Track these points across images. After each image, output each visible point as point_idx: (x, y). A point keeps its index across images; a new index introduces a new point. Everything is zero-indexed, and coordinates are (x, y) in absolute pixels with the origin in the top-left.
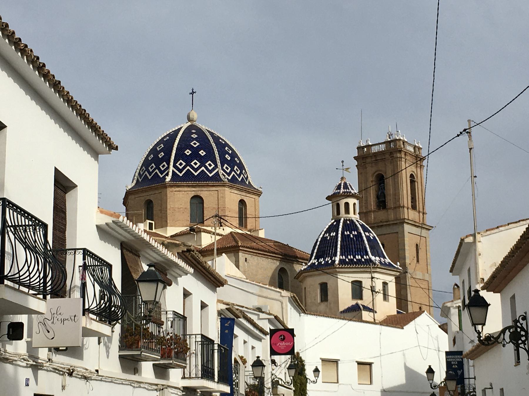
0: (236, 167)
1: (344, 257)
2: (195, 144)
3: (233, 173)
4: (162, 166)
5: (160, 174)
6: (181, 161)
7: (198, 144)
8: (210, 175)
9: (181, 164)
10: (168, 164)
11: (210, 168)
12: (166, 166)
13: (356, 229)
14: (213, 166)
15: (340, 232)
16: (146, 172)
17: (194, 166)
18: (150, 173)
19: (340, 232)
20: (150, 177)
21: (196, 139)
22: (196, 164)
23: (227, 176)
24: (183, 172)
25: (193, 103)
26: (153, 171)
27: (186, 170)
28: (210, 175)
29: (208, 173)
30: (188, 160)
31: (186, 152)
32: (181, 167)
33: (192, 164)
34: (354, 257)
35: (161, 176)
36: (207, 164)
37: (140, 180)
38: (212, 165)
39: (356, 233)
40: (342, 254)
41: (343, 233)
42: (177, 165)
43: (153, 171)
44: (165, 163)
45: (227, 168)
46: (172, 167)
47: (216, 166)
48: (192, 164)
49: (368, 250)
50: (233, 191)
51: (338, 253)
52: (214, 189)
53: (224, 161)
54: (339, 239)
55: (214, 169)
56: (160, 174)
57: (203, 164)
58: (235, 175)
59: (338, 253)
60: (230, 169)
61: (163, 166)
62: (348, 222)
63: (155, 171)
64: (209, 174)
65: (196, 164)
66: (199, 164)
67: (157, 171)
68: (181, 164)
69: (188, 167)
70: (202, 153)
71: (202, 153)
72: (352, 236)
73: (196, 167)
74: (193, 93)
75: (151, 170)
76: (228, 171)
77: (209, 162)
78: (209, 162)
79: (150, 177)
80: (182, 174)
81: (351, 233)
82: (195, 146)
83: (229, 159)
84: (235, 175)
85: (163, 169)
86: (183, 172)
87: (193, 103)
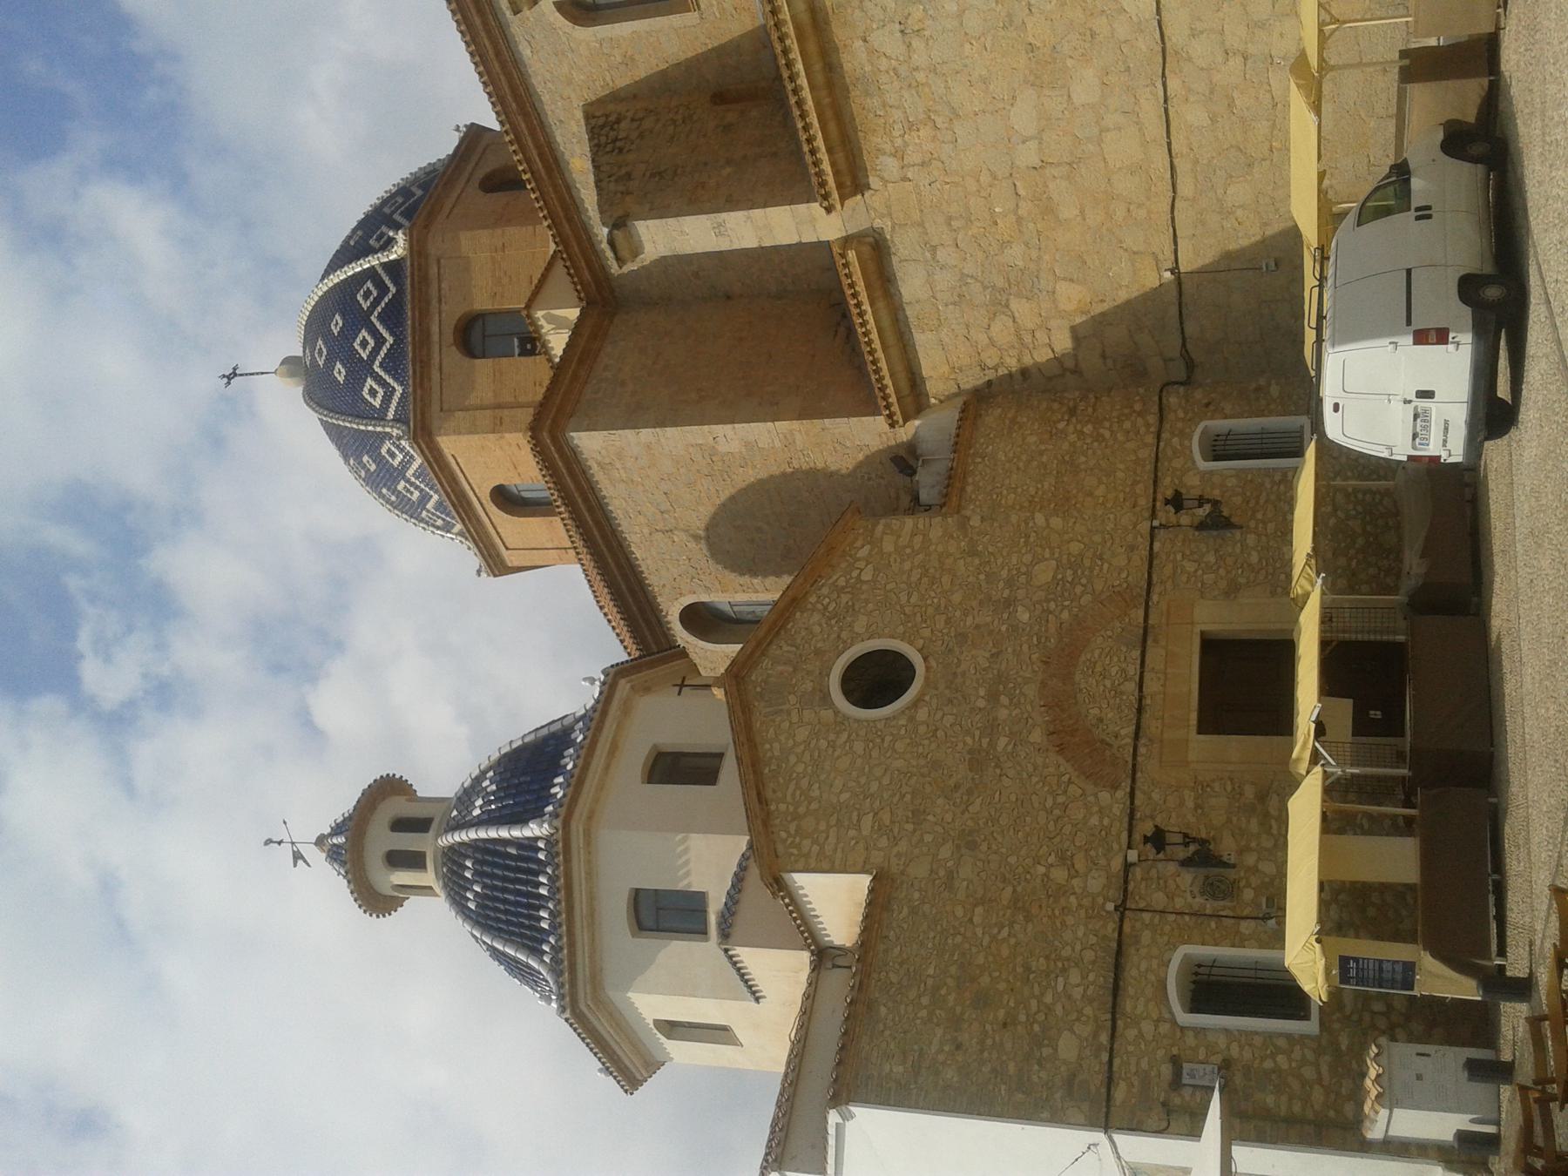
3: (397, 217)
5: (415, 466)
8: (393, 289)
14: (369, 284)
17: (369, 348)
18: (425, 498)
20: (436, 497)
26: (417, 487)
27: (382, 373)
28: (393, 289)
29: (386, 300)
31: (341, 379)
38: (368, 288)
42: (377, 403)
43: (417, 487)
47: (371, 273)
50: (446, 209)
52: (433, 270)
56: (415, 466)
58: (402, 208)
60: (384, 228)
63: (413, 479)
64: (390, 295)
66: (364, 333)
67: (409, 473)
68: (373, 393)
73: (372, 343)
75: (416, 494)
80: (396, 385)
84: (402, 208)
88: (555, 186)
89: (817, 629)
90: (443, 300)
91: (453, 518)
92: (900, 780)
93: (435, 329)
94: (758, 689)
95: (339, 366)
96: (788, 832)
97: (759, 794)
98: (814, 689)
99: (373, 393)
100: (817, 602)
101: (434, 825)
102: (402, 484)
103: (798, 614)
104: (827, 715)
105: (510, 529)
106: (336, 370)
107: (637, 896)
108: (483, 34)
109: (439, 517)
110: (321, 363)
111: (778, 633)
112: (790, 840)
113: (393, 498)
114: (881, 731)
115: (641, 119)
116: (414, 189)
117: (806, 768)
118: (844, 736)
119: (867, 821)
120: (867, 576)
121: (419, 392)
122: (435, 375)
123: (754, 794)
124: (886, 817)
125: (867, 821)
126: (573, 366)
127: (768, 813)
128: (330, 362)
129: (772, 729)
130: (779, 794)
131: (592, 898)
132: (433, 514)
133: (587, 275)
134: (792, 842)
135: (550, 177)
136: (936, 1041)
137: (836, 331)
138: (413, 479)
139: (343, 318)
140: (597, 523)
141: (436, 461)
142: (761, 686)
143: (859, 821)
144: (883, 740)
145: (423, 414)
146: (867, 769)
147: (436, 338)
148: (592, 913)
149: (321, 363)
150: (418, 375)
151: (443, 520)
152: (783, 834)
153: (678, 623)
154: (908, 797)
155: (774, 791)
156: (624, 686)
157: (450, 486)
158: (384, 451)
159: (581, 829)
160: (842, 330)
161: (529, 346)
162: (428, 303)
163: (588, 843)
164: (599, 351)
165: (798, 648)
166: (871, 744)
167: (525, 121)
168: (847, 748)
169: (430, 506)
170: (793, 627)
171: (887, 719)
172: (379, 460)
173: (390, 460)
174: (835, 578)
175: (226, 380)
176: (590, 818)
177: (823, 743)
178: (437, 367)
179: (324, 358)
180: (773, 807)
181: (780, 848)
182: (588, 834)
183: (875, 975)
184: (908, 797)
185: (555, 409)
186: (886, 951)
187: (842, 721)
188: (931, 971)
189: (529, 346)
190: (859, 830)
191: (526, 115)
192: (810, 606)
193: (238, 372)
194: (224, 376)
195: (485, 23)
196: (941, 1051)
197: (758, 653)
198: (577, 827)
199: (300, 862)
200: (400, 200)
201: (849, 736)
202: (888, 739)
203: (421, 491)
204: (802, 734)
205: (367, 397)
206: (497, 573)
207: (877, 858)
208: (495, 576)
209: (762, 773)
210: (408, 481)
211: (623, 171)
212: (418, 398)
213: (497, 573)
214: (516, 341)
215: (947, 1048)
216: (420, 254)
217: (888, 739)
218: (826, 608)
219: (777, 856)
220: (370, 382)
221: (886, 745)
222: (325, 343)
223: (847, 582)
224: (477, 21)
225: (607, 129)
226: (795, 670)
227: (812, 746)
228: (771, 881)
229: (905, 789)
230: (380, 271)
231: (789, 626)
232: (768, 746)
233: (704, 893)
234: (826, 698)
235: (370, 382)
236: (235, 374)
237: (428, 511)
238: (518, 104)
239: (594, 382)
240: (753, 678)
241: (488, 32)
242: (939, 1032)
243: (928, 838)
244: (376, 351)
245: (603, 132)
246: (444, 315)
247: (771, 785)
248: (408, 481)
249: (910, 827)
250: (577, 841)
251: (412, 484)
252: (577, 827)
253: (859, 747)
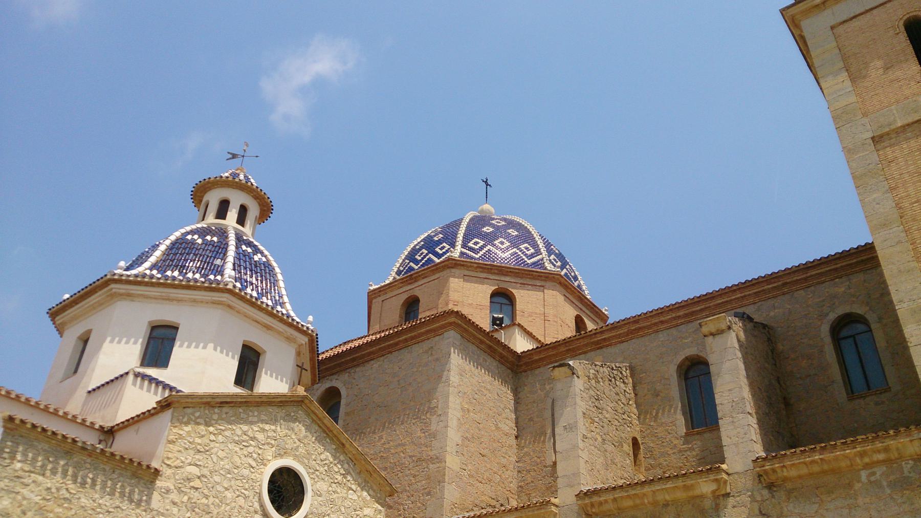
0: (568, 267)
2: (497, 222)
4: (439, 249)
7: (504, 223)
9: (476, 243)
14: (532, 251)
18: (416, 262)
20: (416, 267)
24: (481, 253)
25: (487, 195)
26: (423, 259)
30: (489, 239)
31: (484, 229)
42: (471, 244)
43: (423, 259)
46: (460, 246)
47: (538, 252)
48: (496, 242)
63: (428, 257)
64: (526, 259)
65: (502, 243)
67: (430, 255)
70: (514, 233)
75: (419, 258)
78: (526, 245)
80: (479, 255)
86: (481, 253)
87: (487, 195)
88: (586, 345)
89: (323, 457)
90: (522, 285)
91: (405, 273)
92: (218, 497)
93: (507, 279)
94: (292, 414)
95: (491, 230)
96: (198, 417)
97: (227, 403)
98: (287, 449)
99: (476, 243)
100: (340, 460)
101: (240, 227)
102: (427, 252)
103: (334, 447)
104: (269, 453)
105: (395, 304)
106: (489, 228)
107: (175, 328)
108: (674, 315)
109: (404, 268)
110: (493, 222)
111: (325, 432)
112: (193, 418)
113: (418, 247)
114: (253, 489)
115: (625, 395)
116: (577, 282)
117: (238, 436)
118: (254, 464)
119: (194, 470)
120: (351, 494)
121: (475, 265)
122: (484, 275)
123: (229, 400)
124: (197, 483)
125: (194, 470)
126: (488, 342)
127: (213, 407)
128: (493, 226)
129: (266, 418)
130: (224, 416)
131: (179, 301)
132: (406, 266)
133: (536, 358)
134: (192, 419)
135: (592, 343)
136: (32, 496)
137: (494, 499)
138: (428, 257)
139: (517, 236)
140: (397, 344)
141: (437, 269)
142: (294, 416)
143: (197, 465)
144: (246, 490)
145: (463, 265)
146: (229, 476)
147: (503, 278)
148: (169, 299)
149: (493, 222)
150: (485, 266)
151: (403, 271)
152: (197, 414)
153: (330, 386)
154: (204, 501)
155: (226, 413)
156: (304, 340)
157: (422, 274)
158: (444, 244)
159: (222, 299)
160: (494, 503)
161: (498, 322)
162: (522, 278)
163: (214, 303)
164: (494, 358)
165: (313, 442)
166: (245, 481)
167: (624, 333)
168: (246, 465)
169: (412, 264)
170: (327, 442)
171: (260, 494)
172: (439, 242)
173: (439, 247)
174: (353, 474)
175: (485, 180)
176: (229, 306)
177: (251, 449)
178: (487, 277)
179: (496, 223)
180: (216, 410)
181: (189, 411)
182: (220, 303)
183: (89, 460)
184: (204, 501)
185: (466, 327)
186: (104, 470)
187: (263, 462)
188: (83, 500)
189: (498, 322)
190: (190, 464)
191: (627, 334)
192: (338, 455)
193: (488, 186)
194: (487, 180)
195: (679, 317)
196: (24, 498)
197: (314, 418)
198: (225, 298)
199: (230, 156)
200: (573, 274)
201: (253, 468)
202: (246, 492)
203: (421, 261)
204: (260, 436)
205: (474, 241)
206: (370, 294)
207: (167, 472)
208: (368, 293)
209: (240, 407)
210: (427, 255)
211: (600, 380)
212: (472, 265)
213: (370, 294)
214: (501, 316)
215: (25, 502)
216: (547, 277)
217: (246, 492)
218: (335, 465)
219: (184, 408)
220: (482, 243)
221: (243, 491)
222: (503, 225)
223: (348, 481)
224: (681, 313)
225: (621, 376)
226: (299, 441)
227: (251, 442)
228: (169, 401)
229: (211, 499)
230: (539, 257)
231: (328, 440)
232: (256, 414)
233: (167, 367)
234: (281, 456)
235: (482, 243)
236: (487, 185)
237: (409, 263)
238: (634, 330)
239: (478, 352)
240: (300, 412)
241: (674, 318)
242: (37, 499)
243: (175, 510)
244: (497, 248)
245: (619, 374)
246: (515, 284)
247: (231, 412)
248: (427, 255)
249: (186, 498)
250: (216, 296)
251: (425, 257)
252: (225, 297)
253: (246, 472)
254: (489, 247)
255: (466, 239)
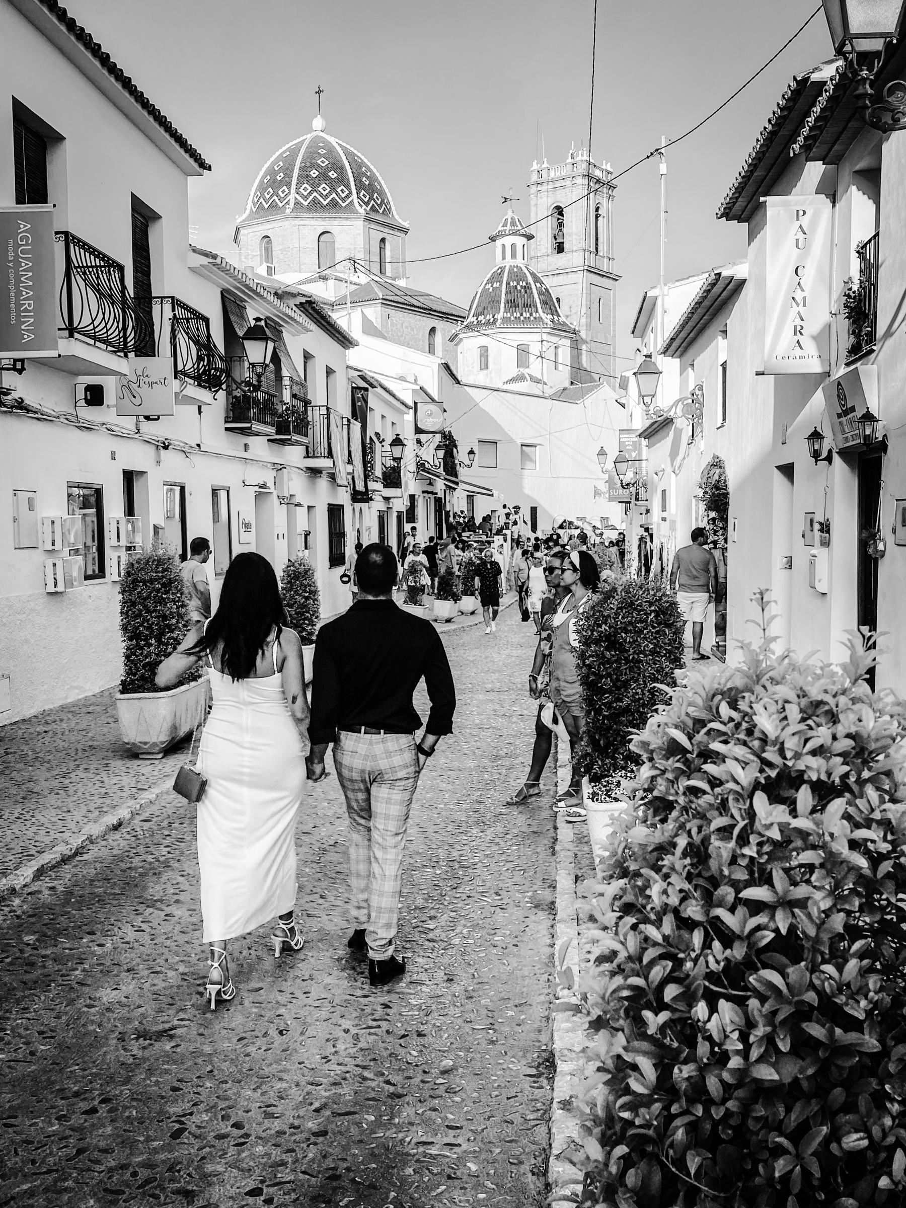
0: (376, 195)
1: (509, 315)
3: (372, 202)
6: (305, 185)
9: (305, 189)
10: (289, 189)
11: (343, 195)
12: (287, 191)
13: (524, 278)
14: (347, 192)
15: (504, 282)
16: (262, 200)
19: (504, 282)
20: (266, 206)
21: (324, 156)
22: (324, 188)
23: (364, 207)
32: (305, 194)
33: (320, 189)
34: (522, 315)
35: (281, 205)
36: (339, 190)
37: (254, 210)
39: (524, 284)
40: (505, 311)
41: (508, 284)
44: (285, 188)
45: (364, 195)
47: (351, 193)
48: (320, 189)
49: (539, 305)
51: (502, 309)
53: (360, 186)
54: (504, 291)
55: (347, 196)
57: (333, 190)
59: (502, 309)
61: (283, 192)
62: (515, 270)
67: (275, 197)
68: (305, 189)
69: (315, 194)
70: (333, 175)
71: (333, 175)
72: (519, 288)
74: (319, 92)
75: (268, 197)
76: (366, 200)
77: (342, 187)
79: (266, 206)
81: (518, 284)
82: (323, 165)
83: (367, 183)
85: (282, 195)
220: (310, 189)
235: (310, 189)
254: (315, 194)
255: (299, 183)
